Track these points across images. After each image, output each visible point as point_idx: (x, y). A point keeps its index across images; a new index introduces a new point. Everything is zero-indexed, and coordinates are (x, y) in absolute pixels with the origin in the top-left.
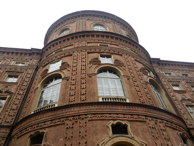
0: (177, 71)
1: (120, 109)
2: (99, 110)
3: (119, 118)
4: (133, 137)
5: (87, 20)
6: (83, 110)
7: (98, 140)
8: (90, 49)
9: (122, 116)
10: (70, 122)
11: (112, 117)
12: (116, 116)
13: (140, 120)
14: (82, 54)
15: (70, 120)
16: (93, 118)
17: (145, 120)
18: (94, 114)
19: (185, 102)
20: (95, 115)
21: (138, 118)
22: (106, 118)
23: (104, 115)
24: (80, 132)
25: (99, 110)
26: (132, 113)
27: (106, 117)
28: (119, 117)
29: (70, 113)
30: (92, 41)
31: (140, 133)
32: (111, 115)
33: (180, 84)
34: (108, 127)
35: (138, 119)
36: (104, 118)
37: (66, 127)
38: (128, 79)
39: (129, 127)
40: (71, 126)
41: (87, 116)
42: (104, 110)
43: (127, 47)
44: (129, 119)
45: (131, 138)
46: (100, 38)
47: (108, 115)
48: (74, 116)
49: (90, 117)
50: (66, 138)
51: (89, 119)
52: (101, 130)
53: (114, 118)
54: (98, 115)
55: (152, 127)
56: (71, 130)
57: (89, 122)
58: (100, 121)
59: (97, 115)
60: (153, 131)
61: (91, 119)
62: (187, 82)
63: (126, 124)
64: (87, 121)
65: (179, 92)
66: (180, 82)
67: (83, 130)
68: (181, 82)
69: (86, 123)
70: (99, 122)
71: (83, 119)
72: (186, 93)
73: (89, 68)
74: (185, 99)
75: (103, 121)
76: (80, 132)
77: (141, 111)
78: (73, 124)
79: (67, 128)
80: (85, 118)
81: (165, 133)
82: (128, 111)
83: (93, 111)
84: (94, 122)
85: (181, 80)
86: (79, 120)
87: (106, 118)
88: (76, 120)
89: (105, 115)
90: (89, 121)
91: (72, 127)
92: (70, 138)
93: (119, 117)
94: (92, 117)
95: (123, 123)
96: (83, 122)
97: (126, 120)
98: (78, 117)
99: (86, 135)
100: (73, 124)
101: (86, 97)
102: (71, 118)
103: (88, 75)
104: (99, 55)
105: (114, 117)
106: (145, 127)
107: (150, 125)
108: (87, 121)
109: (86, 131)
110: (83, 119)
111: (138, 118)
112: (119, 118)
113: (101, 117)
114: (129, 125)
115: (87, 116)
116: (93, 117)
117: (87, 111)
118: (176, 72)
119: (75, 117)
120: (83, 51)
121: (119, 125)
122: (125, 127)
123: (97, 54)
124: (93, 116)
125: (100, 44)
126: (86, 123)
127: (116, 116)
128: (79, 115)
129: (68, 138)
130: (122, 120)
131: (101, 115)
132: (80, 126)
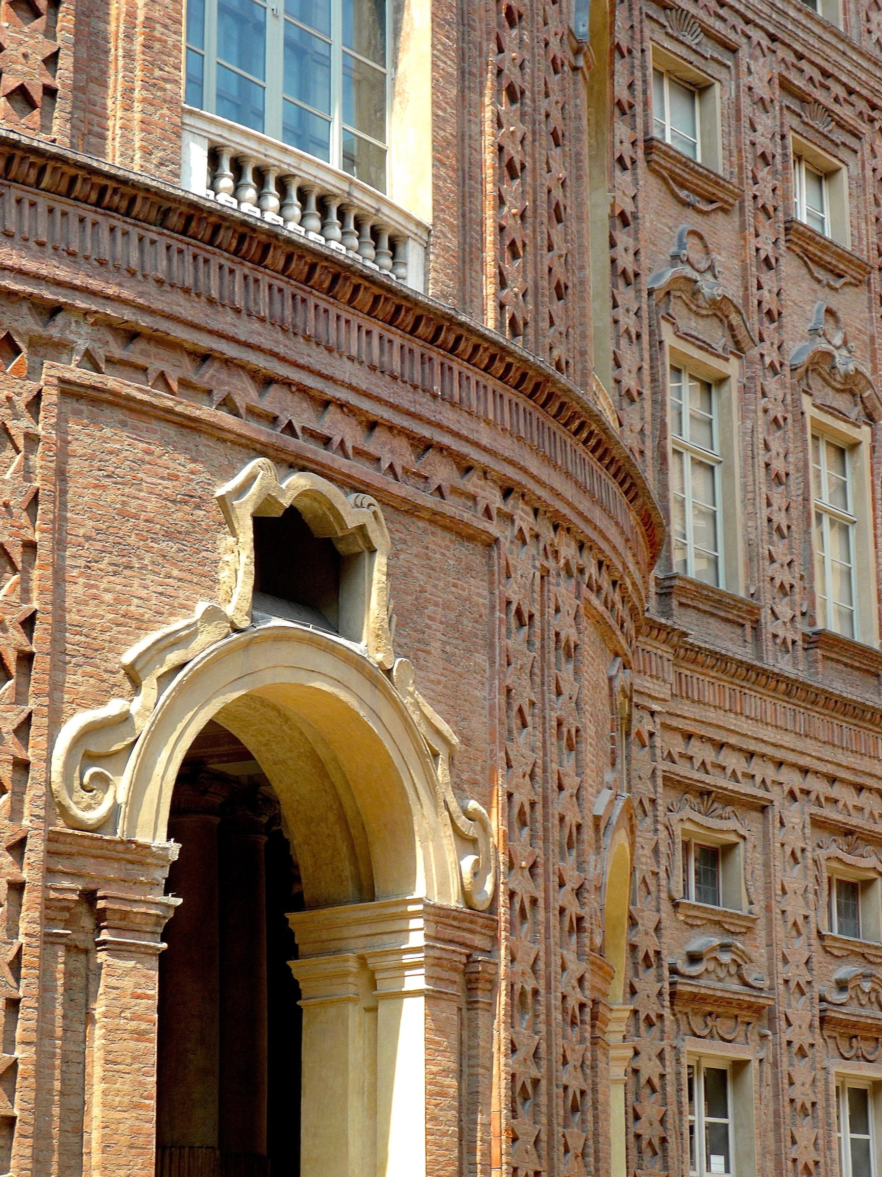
3: (324, 455)
17: (493, 528)
19: (683, 327)
20: (134, 353)
21: (455, 491)
23: (209, 374)
26: (426, 432)
28: (326, 441)
31: (435, 646)
32: (272, 401)
33: (723, 74)
35: (452, 507)
36: (206, 412)
39: (378, 571)
41: (54, 332)
42: (225, 321)
45: (374, 682)
47: (246, 393)
49: (82, 345)
52: (169, 536)
54: (158, 361)
55: (519, 613)
59: (152, 349)
61: (90, 377)
62: (785, 85)
63: (362, 528)
65: (682, 186)
66: (733, 50)
68: (744, 52)
74: (696, 293)
77: (487, 423)
80: (34, 343)
82: (404, 397)
89: (224, 375)
93: (326, 441)
94: (100, 354)
95: (353, 512)
101: (52, 61)
106: (477, 589)
108: (51, 396)
111: (455, 491)
112: (324, 455)
114: (380, 537)
116: (109, 361)
124: (118, 351)
127: (302, 416)
131: (186, 369)
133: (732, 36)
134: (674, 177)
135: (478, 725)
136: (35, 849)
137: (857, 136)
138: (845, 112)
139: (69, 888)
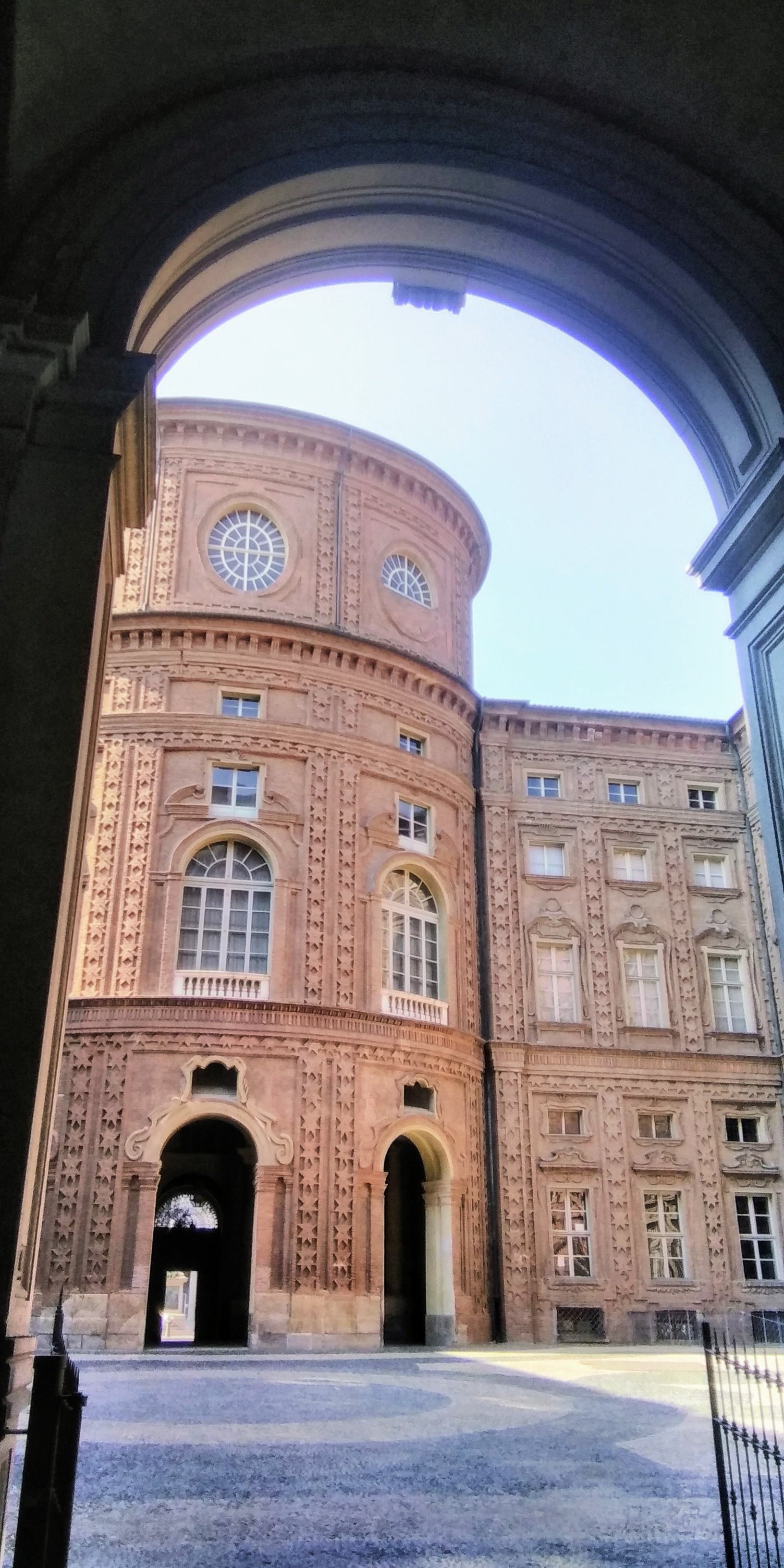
0: (593, 765)
1: (229, 1021)
2: (168, 1024)
3: (218, 1049)
4: (245, 1104)
5: (188, 472)
6: (120, 1019)
7: (151, 1107)
8: (176, 727)
9: (230, 1041)
10: (84, 1050)
11: (201, 1045)
12: (214, 1040)
13: (281, 1052)
14: (140, 755)
15: (85, 1045)
16: (147, 1047)
17: (296, 1054)
18: (153, 1034)
20: (154, 1039)
22: (183, 1048)
24: (107, 1083)
25: (168, 1024)
27: (184, 1044)
29: (85, 1025)
30: (192, 672)
34: (183, 1076)
36: (175, 1048)
37: (71, 1066)
38: (294, 894)
40: (87, 1063)
43: (349, 692)
44: (248, 1052)
46: (230, 654)
47: (190, 1040)
48: (95, 1035)
50: (72, 1094)
51: (135, 1047)
53: (206, 1049)
54: (160, 1039)
56: (82, 1077)
57: (136, 1056)
58: (165, 1056)
60: (310, 1085)
61: (141, 1048)
64: (130, 1054)
65: (545, 883)
67: (115, 1080)
69: (125, 1058)
70: (161, 1058)
71: (118, 1046)
72: (571, 885)
73: (161, 837)
75: (171, 1056)
76: (107, 1083)
77: (291, 1025)
78: (90, 1059)
79: (75, 1068)
81: (346, 1089)
83: (150, 1024)
84: (147, 1057)
85: (585, 820)
86: (107, 1049)
87: (183, 1048)
88: (101, 1049)
90: (135, 1052)
91: (89, 1068)
92: (82, 1097)
95: (228, 1063)
96: (117, 1055)
97: (238, 1055)
98: (104, 1039)
99: (122, 1093)
100: (90, 1059)
102: (85, 1040)
103: (154, 877)
104: (211, 762)
105: (206, 1046)
106: (290, 1073)
107: (308, 1070)
109: (124, 1082)
110: (118, 1046)
113: (167, 1041)
115: (130, 1039)
117: (131, 1023)
118: (585, 770)
119: (97, 1039)
120: (145, 737)
121: (216, 1067)
122: (233, 1072)
123: (200, 755)
124: (148, 1039)
125: (225, 688)
126: (125, 1058)
128: (110, 1035)
129: (76, 1095)
130: (229, 1055)
131: (170, 1038)
132: (109, 1067)
133: (572, 825)
134: (541, 883)
135: (289, 1111)
136: (120, 1168)
137: (655, 835)
138: (647, 830)
139: (129, 1176)
